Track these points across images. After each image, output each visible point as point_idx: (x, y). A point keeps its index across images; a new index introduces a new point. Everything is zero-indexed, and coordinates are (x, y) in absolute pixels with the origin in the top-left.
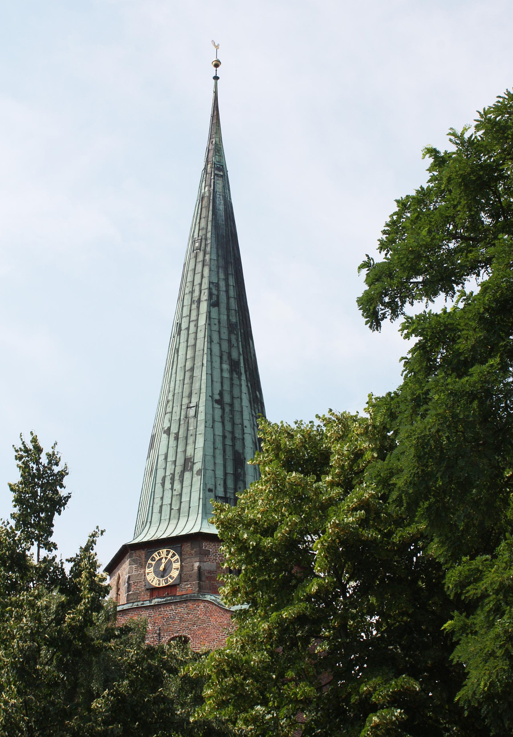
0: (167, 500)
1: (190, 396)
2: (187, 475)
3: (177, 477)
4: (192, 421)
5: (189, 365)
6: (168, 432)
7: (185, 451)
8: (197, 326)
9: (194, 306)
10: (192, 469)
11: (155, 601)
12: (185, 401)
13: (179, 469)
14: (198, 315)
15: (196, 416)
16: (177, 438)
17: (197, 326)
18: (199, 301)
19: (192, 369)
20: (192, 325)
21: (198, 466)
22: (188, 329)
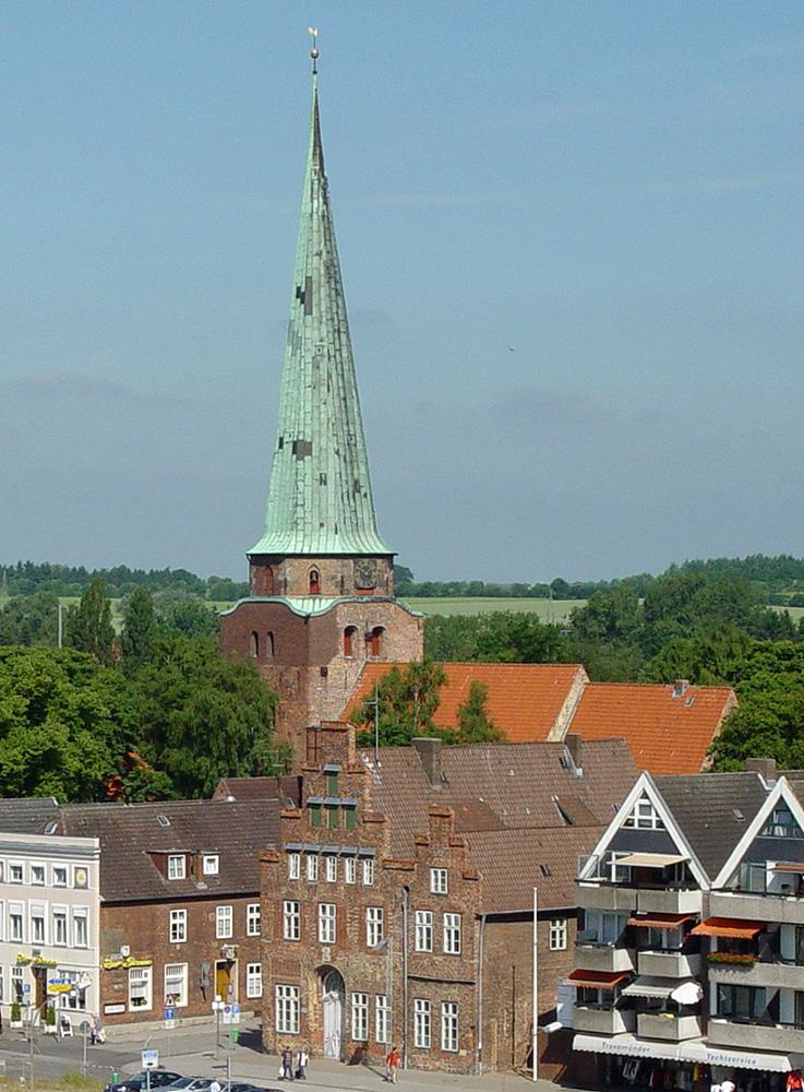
0: (348, 515)
1: (348, 423)
2: (357, 494)
3: (351, 496)
4: (353, 448)
5: (342, 396)
6: (337, 452)
7: (352, 474)
8: (341, 356)
9: (336, 335)
10: (359, 492)
11: (366, 599)
12: (345, 428)
13: (351, 489)
14: (340, 345)
15: (355, 445)
16: (345, 461)
17: (341, 356)
18: (339, 332)
19: (345, 399)
20: (338, 353)
21: (363, 491)
22: (335, 356)
